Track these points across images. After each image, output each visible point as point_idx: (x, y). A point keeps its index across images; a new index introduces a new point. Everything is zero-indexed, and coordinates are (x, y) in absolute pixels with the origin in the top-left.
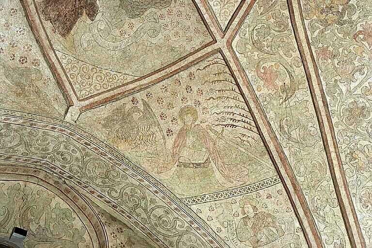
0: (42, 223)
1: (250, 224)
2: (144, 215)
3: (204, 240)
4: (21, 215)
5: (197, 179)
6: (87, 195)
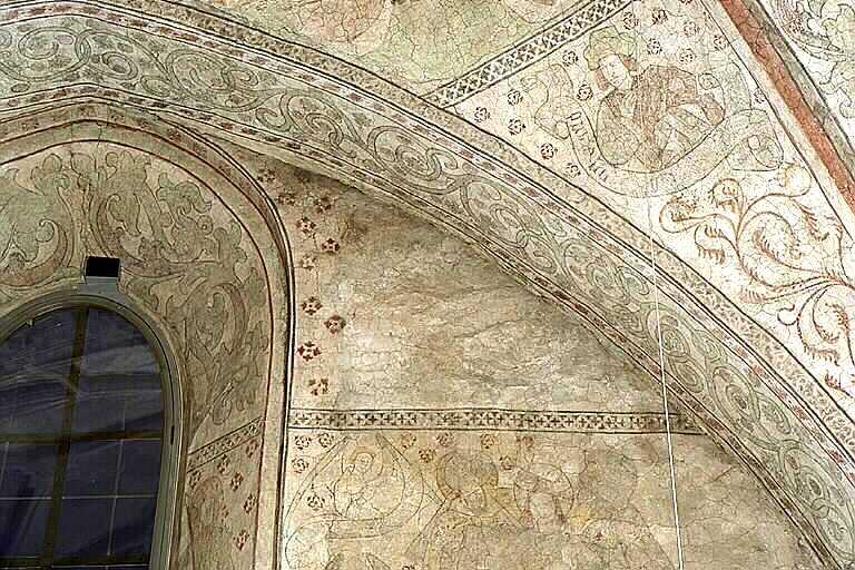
0: (147, 233)
1: (627, 111)
2: (362, 154)
3: (515, 192)
4: (95, 225)
5: (456, 22)
6: (220, 134)
